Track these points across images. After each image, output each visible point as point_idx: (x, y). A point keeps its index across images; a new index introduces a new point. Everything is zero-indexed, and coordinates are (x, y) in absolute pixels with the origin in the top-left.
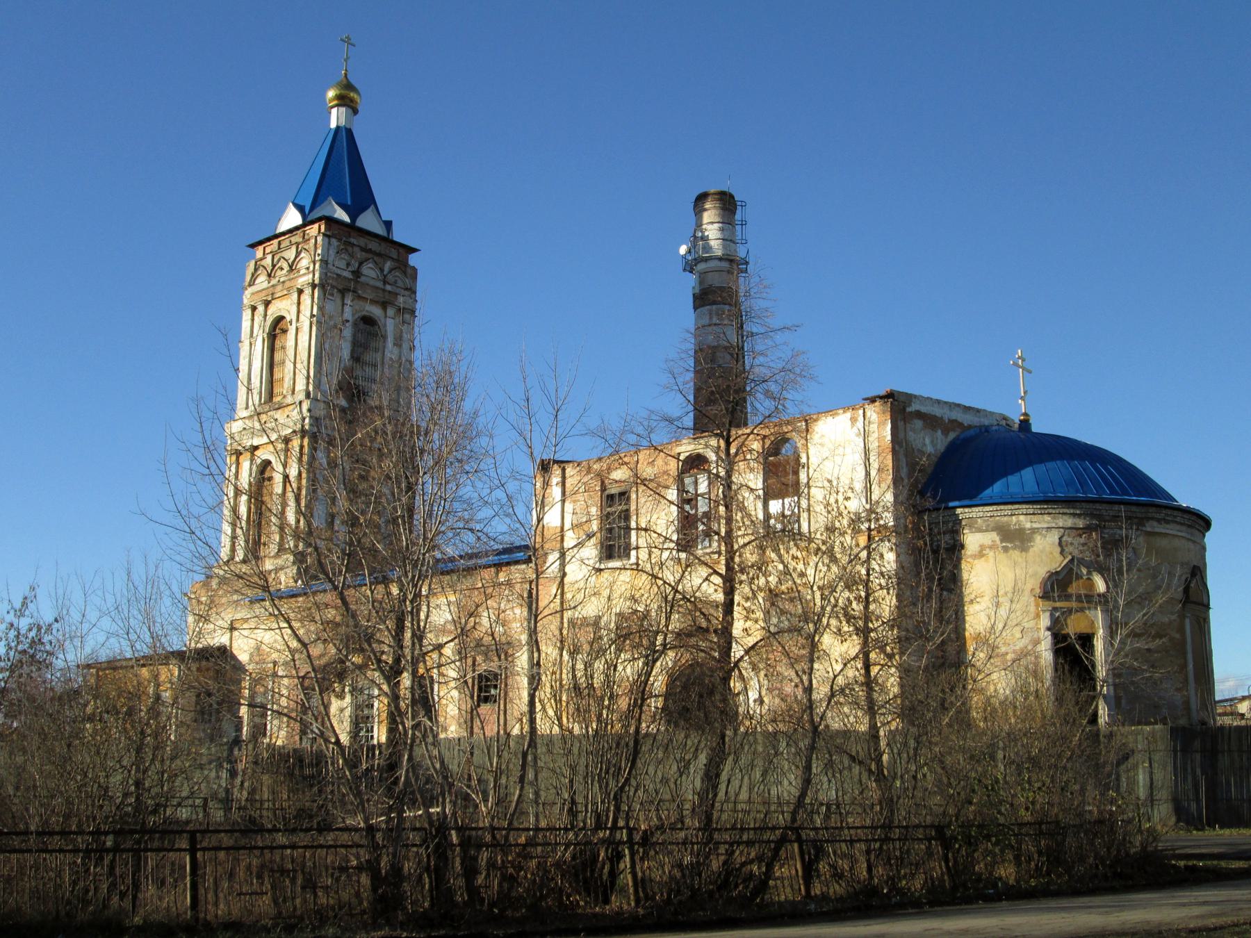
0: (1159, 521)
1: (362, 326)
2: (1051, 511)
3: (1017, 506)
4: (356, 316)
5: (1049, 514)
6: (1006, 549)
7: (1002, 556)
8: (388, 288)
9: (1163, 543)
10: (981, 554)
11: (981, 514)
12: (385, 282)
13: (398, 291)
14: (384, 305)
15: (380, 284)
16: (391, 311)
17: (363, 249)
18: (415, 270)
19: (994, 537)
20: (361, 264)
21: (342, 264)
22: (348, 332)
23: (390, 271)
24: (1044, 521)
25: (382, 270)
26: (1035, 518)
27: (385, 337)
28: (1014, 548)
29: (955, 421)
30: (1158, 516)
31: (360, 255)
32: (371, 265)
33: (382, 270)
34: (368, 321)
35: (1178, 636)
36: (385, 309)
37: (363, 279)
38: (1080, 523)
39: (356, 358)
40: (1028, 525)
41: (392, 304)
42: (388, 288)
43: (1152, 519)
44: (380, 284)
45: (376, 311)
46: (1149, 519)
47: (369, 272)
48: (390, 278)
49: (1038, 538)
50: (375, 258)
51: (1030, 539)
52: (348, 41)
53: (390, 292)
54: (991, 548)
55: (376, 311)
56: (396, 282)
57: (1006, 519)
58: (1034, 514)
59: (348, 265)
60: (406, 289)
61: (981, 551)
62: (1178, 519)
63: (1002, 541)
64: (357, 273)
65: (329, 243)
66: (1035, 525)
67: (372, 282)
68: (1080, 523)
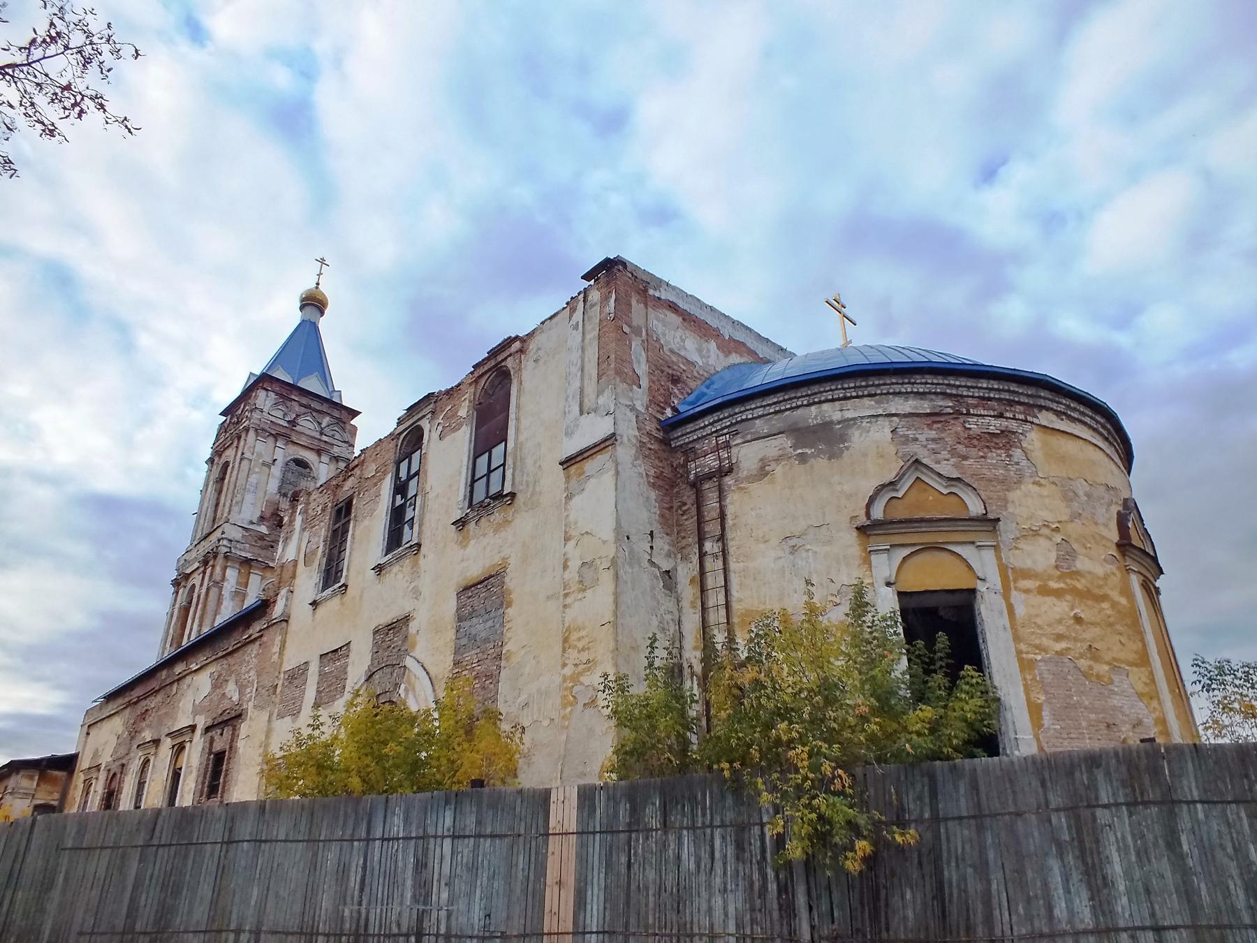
0: (1058, 414)
1: (292, 465)
2: (872, 390)
3: (816, 389)
5: (870, 395)
6: (803, 459)
7: (798, 469)
8: (325, 438)
9: (1070, 446)
10: (763, 472)
11: (760, 412)
12: (321, 434)
13: (335, 442)
14: (319, 452)
15: (317, 435)
16: (325, 458)
17: (301, 405)
18: (355, 428)
19: (785, 442)
21: (280, 414)
22: (277, 471)
24: (866, 407)
25: (320, 424)
26: (849, 403)
28: (820, 452)
29: (743, 344)
30: (1054, 406)
31: (297, 408)
33: (320, 424)
34: (301, 463)
35: (1123, 601)
36: (319, 455)
37: (298, 428)
38: (925, 406)
40: (837, 416)
41: (327, 452)
42: (325, 438)
43: (1048, 409)
44: (317, 435)
45: (310, 457)
46: (1041, 408)
47: (307, 425)
48: (326, 431)
49: (856, 436)
50: (314, 414)
51: (843, 438)
52: (322, 261)
53: (325, 442)
54: (778, 460)
55: (310, 457)
57: (800, 411)
58: (845, 398)
59: (285, 415)
60: (345, 442)
61: (762, 468)
62: (1087, 420)
63: (795, 447)
64: (293, 423)
65: (267, 396)
66: (849, 415)
67: (308, 432)
68: (925, 406)
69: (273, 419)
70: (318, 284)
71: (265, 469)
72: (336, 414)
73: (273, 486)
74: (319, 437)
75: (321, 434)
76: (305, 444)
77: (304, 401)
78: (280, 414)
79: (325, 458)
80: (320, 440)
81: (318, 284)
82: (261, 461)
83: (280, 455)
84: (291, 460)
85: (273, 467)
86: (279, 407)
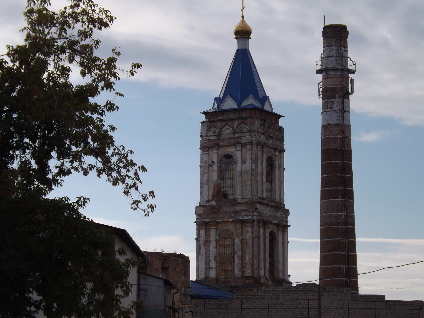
4: (221, 157)
8: (237, 135)
14: (235, 145)
16: (239, 148)
17: (221, 121)
20: (221, 129)
22: (215, 167)
23: (237, 127)
25: (233, 128)
27: (235, 162)
32: (227, 127)
34: (229, 156)
37: (222, 136)
39: (221, 177)
42: (237, 135)
44: (232, 136)
45: (231, 150)
47: (227, 131)
53: (237, 137)
55: (231, 150)
56: (242, 130)
60: (248, 132)
64: (219, 135)
65: (204, 126)
67: (227, 136)
69: (209, 138)
70: (243, 17)
71: (210, 168)
72: (244, 115)
73: (215, 176)
74: (233, 136)
75: (235, 133)
76: (227, 144)
77: (226, 116)
78: (211, 134)
79: (239, 148)
80: (234, 138)
81: (243, 17)
82: (207, 165)
83: (215, 158)
84: (222, 157)
85: (213, 165)
86: (211, 129)
